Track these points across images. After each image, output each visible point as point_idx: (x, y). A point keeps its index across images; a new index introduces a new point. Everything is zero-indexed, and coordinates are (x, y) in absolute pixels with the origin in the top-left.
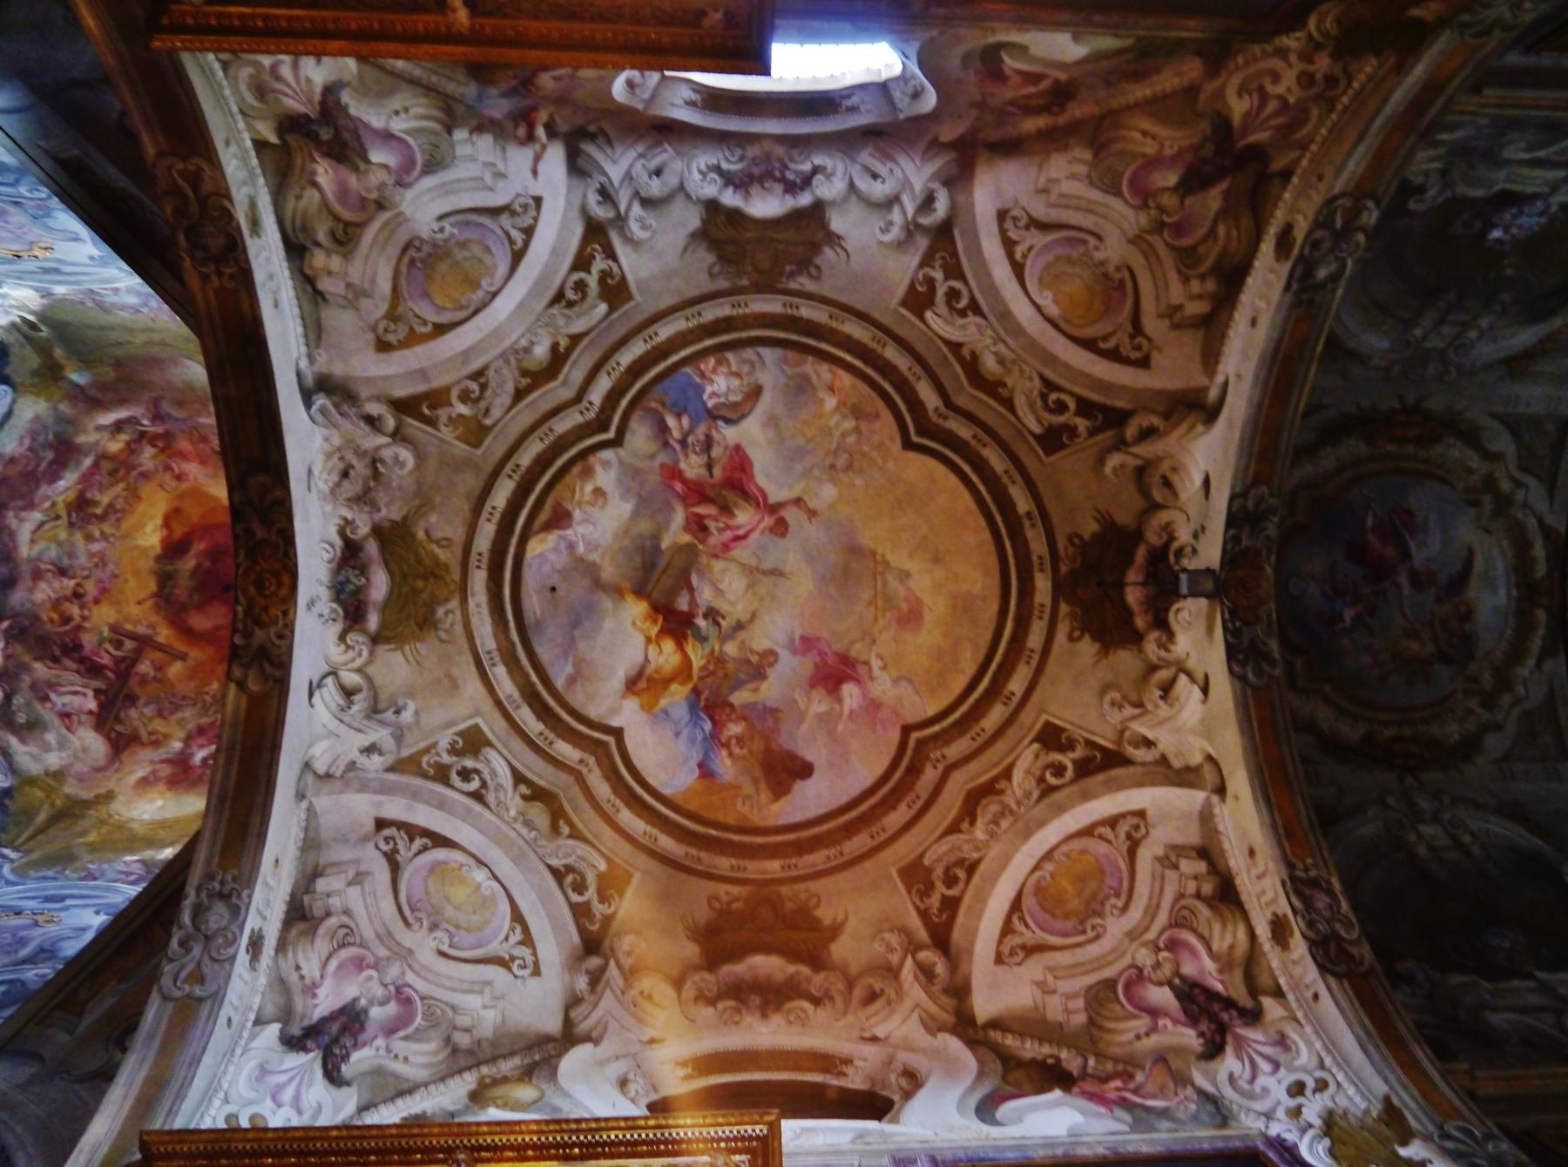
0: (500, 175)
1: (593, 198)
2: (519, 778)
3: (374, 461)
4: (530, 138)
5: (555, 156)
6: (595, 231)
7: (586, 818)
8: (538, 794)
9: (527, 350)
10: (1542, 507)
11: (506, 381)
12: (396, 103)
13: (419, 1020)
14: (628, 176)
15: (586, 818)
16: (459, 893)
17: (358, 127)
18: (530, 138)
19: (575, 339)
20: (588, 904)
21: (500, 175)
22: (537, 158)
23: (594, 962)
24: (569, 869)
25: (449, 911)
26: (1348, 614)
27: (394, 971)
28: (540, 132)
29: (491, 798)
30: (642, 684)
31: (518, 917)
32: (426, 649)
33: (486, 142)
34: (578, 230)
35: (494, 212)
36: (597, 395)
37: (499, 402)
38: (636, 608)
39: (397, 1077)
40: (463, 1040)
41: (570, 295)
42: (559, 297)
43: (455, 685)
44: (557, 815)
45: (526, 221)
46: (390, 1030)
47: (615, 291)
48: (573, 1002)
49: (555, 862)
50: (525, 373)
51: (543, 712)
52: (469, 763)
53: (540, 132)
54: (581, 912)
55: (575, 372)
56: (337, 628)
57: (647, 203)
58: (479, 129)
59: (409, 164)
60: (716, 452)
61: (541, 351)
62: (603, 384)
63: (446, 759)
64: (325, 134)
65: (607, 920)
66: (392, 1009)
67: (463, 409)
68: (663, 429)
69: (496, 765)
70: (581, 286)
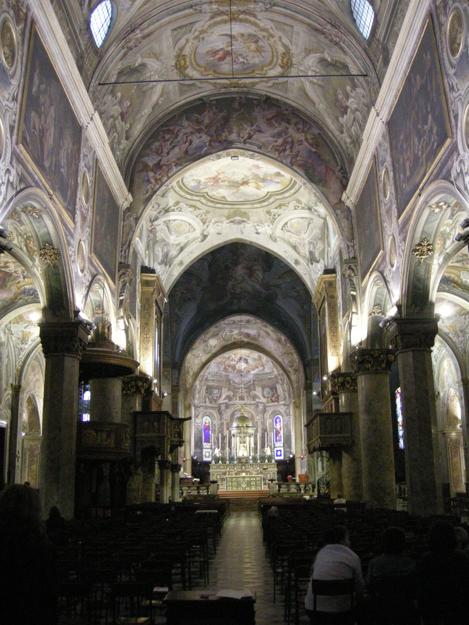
0: (162, 230)
1: (161, 214)
2: (276, 208)
3: (215, 223)
4: (154, 228)
5: (155, 223)
6: (167, 211)
7: (285, 201)
8: (280, 206)
9: (191, 211)
10: (202, 23)
11: (198, 212)
12: (157, 252)
13: (315, 242)
14: (155, 211)
15: (285, 201)
16: (296, 226)
17: (163, 256)
18: (154, 228)
19: (187, 205)
20: (302, 207)
21: (162, 230)
22: (157, 225)
23: (313, 210)
24: (295, 207)
25: (298, 229)
26: (241, 60)
27: (306, 242)
28: (153, 227)
29: (280, 214)
30: (258, 188)
31: (302, 218)
32: (250, 214)
33: (157, 235)
34: (167, 214)
35: (168, 227)
36: (198, 198)
37: (201, 211)
38: (242, 188)
39: (322, 251)
40: (320, 236)
41: (179, 209)
42: (180, 211)
43: (257, 212)
44: (284, 205)
45: (168, 222)
46: (314, 248)
47: (177, 203)
48: (319, 216)
49: (293, 208)
50: (195, 210)
51: (264, 201)
52: (273, 214)
53: (153, 227)
54: (303, 208)
55: (193, 203)
56: (246, 224)
57: (159, 206)
58: (156, 237)
59: (165, 244)
60: (207, 181)
61: (191, 209)
62: (195, 198)
63: (271, 217)
64: (166, 260)
65: (305, 205)
66: (311, 246)
67: (204, 216)
68: (203, 188)
69: (273, 211)
70: (177, 209)
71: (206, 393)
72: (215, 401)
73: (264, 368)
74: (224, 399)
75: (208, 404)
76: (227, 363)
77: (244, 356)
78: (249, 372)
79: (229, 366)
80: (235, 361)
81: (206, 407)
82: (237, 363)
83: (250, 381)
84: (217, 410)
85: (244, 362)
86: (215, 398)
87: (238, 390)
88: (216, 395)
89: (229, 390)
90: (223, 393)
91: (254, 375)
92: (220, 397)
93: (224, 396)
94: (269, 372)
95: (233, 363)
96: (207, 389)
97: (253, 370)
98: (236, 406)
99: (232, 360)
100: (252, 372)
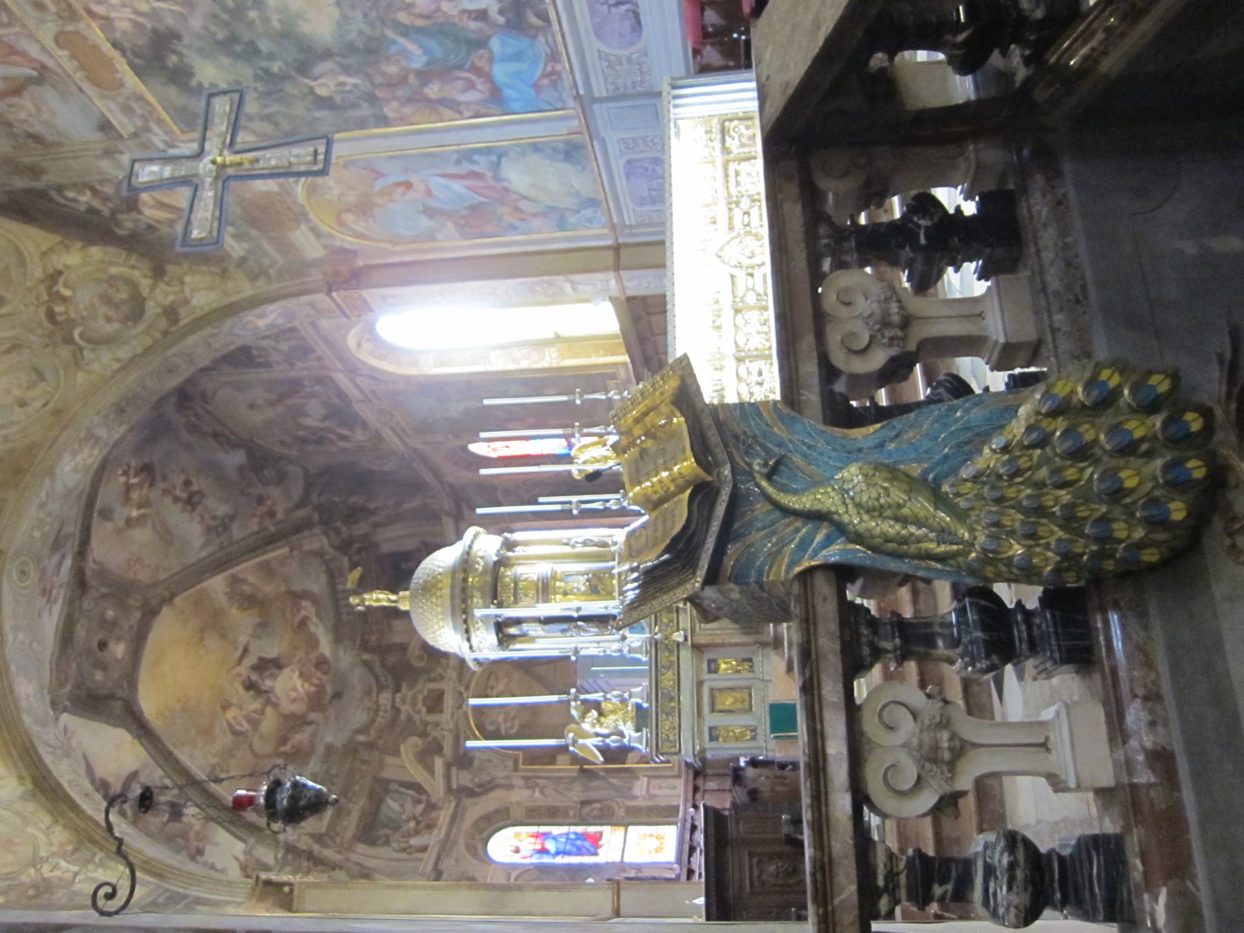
71: (387, 843)
72: (432, 807)
73: (305, 595)
74: (431, 771)
75: (433, 839)
76: (268, 748)
77: (244, 670)
78: (321, 663)
79: (284, 740)
80: (262, 712)
81: (446, 845)
82: (276, 706)
83: (367, 664)
84: (468, 802)
85: (274, 677)
86: (420, 808)
87: (403, 717)
88: (409, 806)
89: (396, 752)
90: (407, 779)
91: (337, 640)
92: (417, 787)
93: (417, 774)
94: (323, 578)
95: (270, 722)
96: (372, 842)
97: (313, 643)
98: (462, 724)
99: (255, 724)
100: (326, 648)
